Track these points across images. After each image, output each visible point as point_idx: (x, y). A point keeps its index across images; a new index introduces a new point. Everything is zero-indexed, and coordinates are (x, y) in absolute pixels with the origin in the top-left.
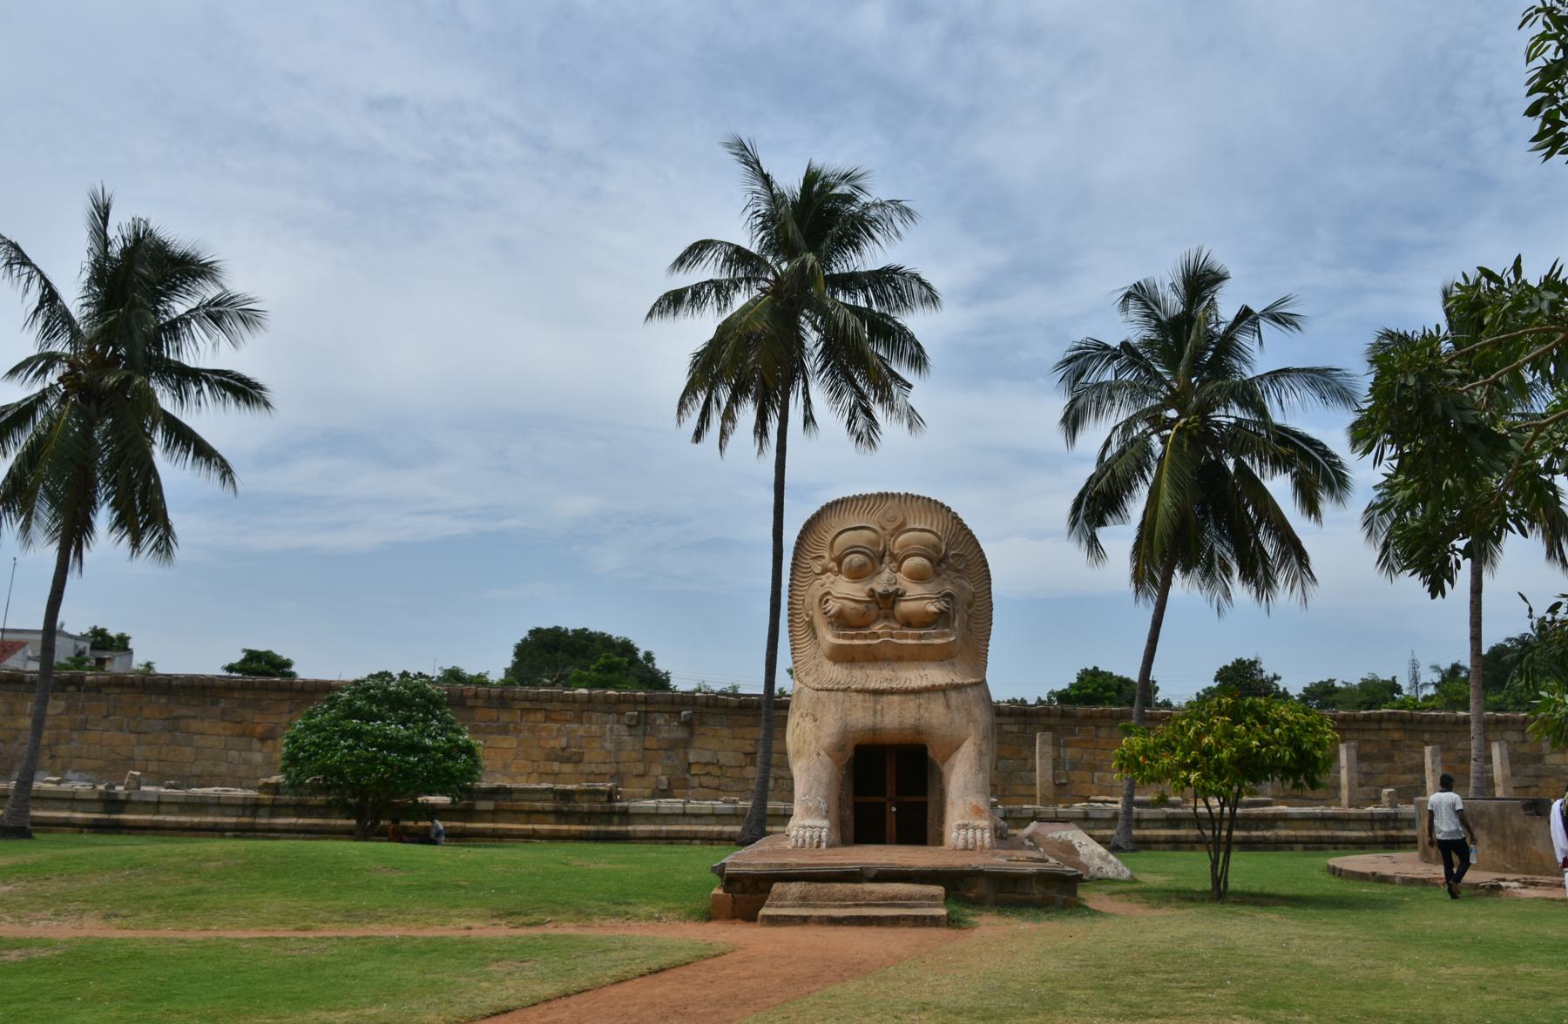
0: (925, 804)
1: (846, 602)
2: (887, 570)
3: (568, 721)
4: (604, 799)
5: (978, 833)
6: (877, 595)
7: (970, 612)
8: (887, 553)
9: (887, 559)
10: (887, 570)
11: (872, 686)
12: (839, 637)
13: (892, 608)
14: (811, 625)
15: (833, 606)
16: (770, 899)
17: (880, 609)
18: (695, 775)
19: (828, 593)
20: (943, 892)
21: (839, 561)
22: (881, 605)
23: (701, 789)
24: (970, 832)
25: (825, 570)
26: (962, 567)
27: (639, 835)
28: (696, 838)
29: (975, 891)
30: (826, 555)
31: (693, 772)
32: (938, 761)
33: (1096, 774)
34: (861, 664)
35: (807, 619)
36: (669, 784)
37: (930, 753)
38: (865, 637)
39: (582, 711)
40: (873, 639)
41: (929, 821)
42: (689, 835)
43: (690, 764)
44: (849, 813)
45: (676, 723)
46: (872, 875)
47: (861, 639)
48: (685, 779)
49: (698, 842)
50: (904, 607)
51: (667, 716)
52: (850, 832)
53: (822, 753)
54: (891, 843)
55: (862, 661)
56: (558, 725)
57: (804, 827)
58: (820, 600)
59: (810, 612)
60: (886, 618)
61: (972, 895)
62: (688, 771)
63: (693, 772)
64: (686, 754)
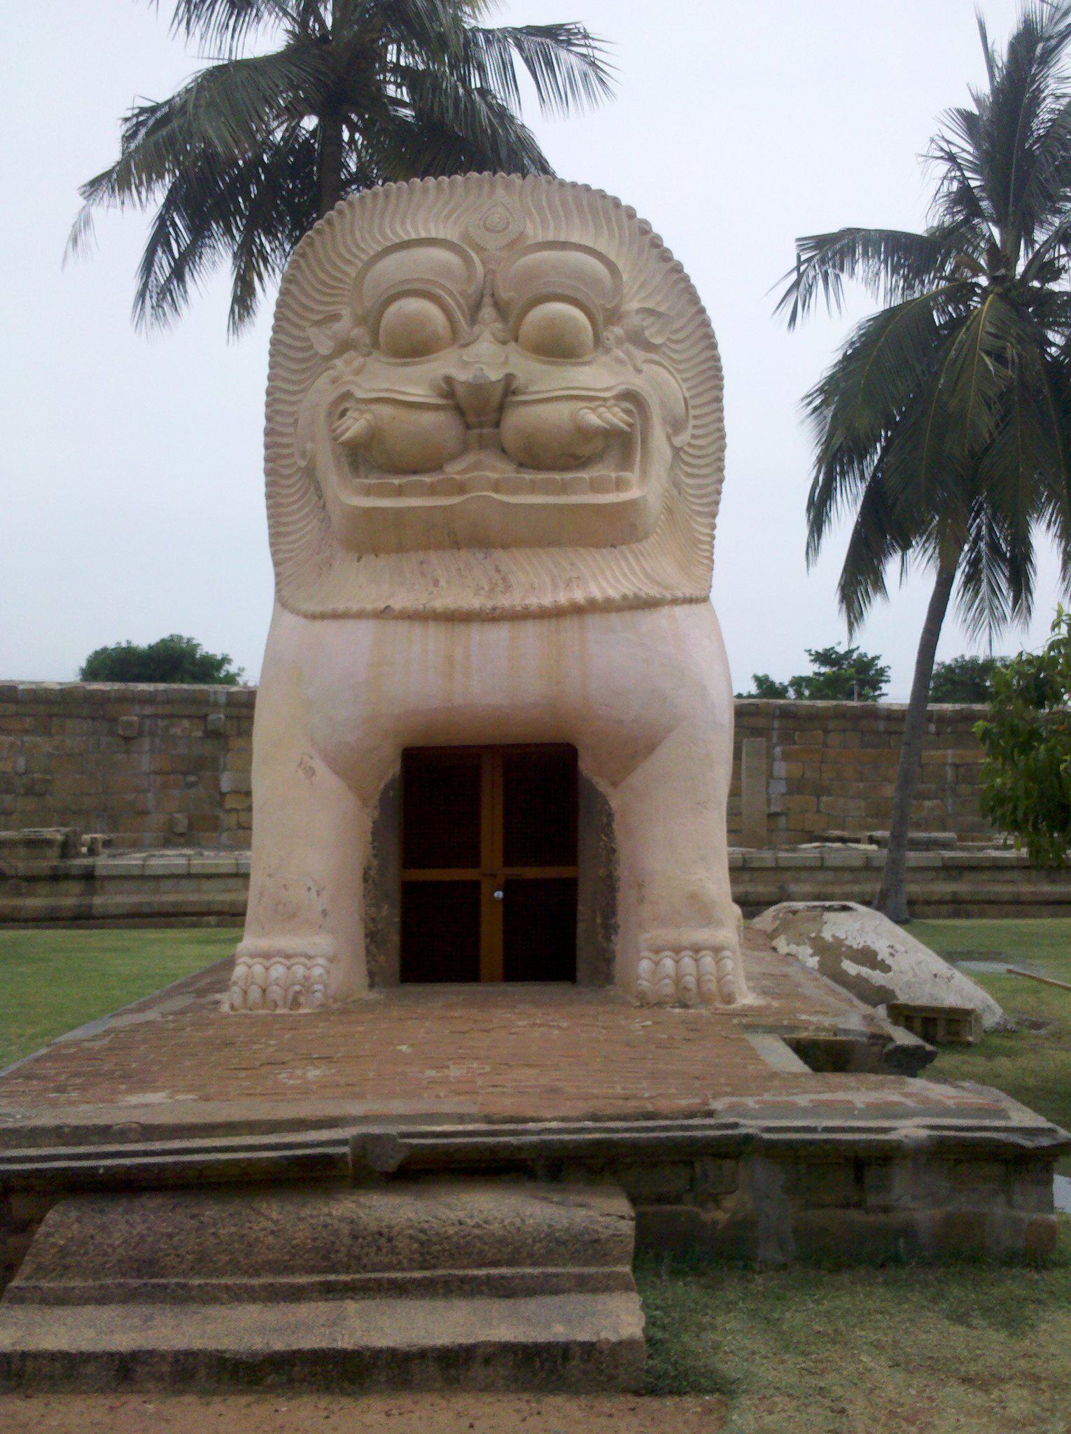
0: (571, 886)
1: (386, 411)
2: (487, 335)
3: (27, 732)
4: (56, 851)
5: (708, 960)
6: (460, 391)
7: (679, 440)
8: (487, 300)
9: (488, 312)
10: (487, 335)
11: (443, 602)
12: (368, 491)
13: (497, 424)
14: (310, 473)
15: (354, 426)
16: (27, 1268)
17: (468, 426)
18: (231, 810)
19: (347, 396)
20: (627, 1227)
21: (372, 320)
22: (472, 419)
23: (240, 832)
24: (687, 961)
25: (344, 346)
26: (658, 341)
27: (113, 911)
28: (209, 913)
29: (729, 1202)
30: (346, 312)
31: (228, 806)
32: (602, 786)
33: (824, 799)
34: (421, 555)
35: (303, 464)
36: (191, 825)
37: (586, 766)
38: (432, 490)
39: (50, 716)
40: (448, 493)
41: (581, 927)
42: (197, 909)
43: (223, 795)
44: (390, 913)
45: (200, 734)
46: (392, 1165)
47: (422, 495)
48: (217, 818)
49: (212, 919)
50: (519, 419)
51: (186, 723)
52: (391, 960)
53: (319, 766)
54: (492, 979)
55: (426, 548)
56: (11, 738)
57: (267, 956)
58: (330, 414)
59: (309, 446)
60: (482, 445)
61: (721, 1216)
62: (221, 804)
63: (228, 806)
64: (217, 780)
